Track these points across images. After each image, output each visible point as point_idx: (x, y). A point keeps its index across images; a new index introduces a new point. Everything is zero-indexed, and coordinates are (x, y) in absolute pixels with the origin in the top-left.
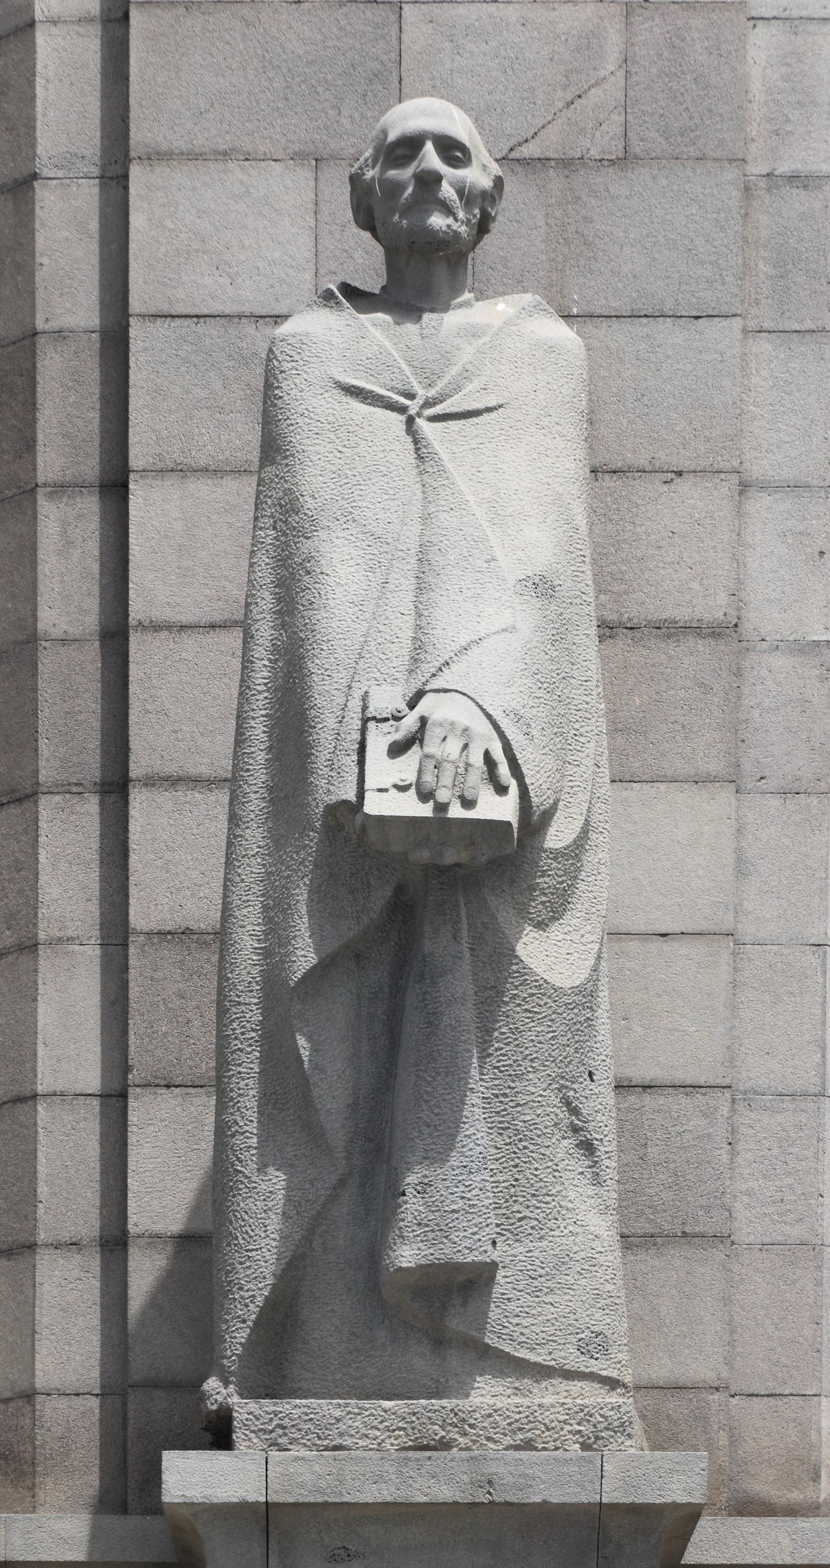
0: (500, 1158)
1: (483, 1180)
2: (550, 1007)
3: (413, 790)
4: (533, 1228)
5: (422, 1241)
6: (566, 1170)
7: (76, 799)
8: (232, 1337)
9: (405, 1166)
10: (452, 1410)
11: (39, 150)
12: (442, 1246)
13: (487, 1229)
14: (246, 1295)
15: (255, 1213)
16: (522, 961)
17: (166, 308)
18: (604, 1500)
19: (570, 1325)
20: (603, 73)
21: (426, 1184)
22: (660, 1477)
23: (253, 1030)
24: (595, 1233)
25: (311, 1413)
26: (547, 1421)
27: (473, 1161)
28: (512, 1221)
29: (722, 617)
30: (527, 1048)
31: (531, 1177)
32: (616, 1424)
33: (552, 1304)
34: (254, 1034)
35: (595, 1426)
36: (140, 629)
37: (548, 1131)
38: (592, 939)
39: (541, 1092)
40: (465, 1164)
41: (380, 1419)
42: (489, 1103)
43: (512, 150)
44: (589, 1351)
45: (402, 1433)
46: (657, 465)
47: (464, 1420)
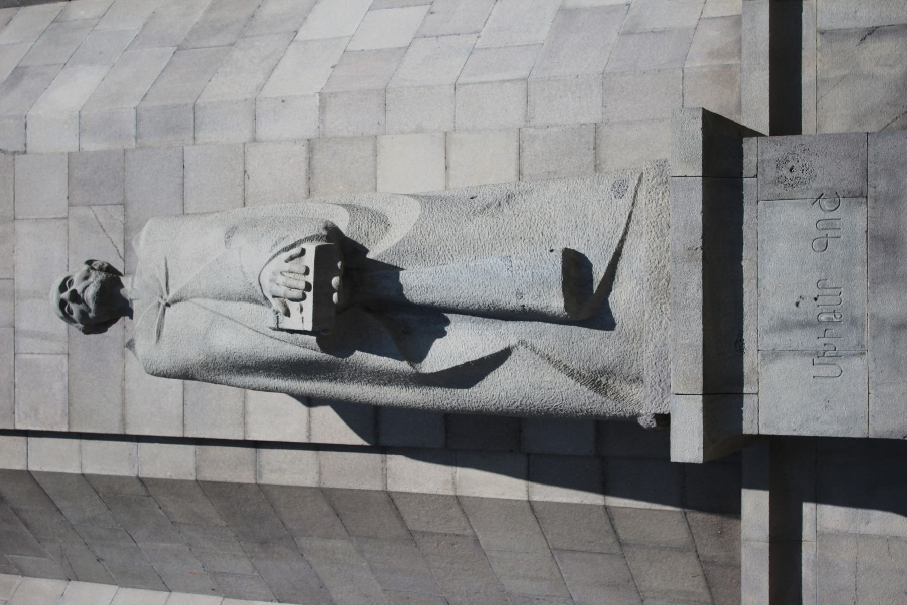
0: (509, 249)
1: (516, 258)
2: (429, 221)
3: (303, 303)
4: (548, 228)
5: (549, 294)
6: (520, 210)
7: (389, 472)
8: (613, 411)
9: (508, 305)
10: (650, 275)
11: (127, 474)
12: (552, 282)
13: (544, 255)
14: (587, 402)
15: (542, 394)
16: (403, 239)
17: (181, 419)
18: (701, 175)
19: (606, 204)
20: (93, 216)
21: (517, 293)
22: (686, 139)
23: (446, 393)
24: (557, 191)
25: (651, 364)
26: (657, 214)
27: (506, 265)
28: (544, 241)
29: (305, 147)
30: (449, 235)
31: (520, 229)
32: (658, 171)
33: (593, 215)
34: (449, 393)
35: (659, 184)
36: (310, 437)
37: (495, 220)
38: (402, 200)
39: (474, 225)
40: (507, 269)
41: (655, 320)
42: (478, 256)
43: (121, 257)
44: (622, 191)
45: (663, 306)
46: (242, 183)
47: (656, 268)
